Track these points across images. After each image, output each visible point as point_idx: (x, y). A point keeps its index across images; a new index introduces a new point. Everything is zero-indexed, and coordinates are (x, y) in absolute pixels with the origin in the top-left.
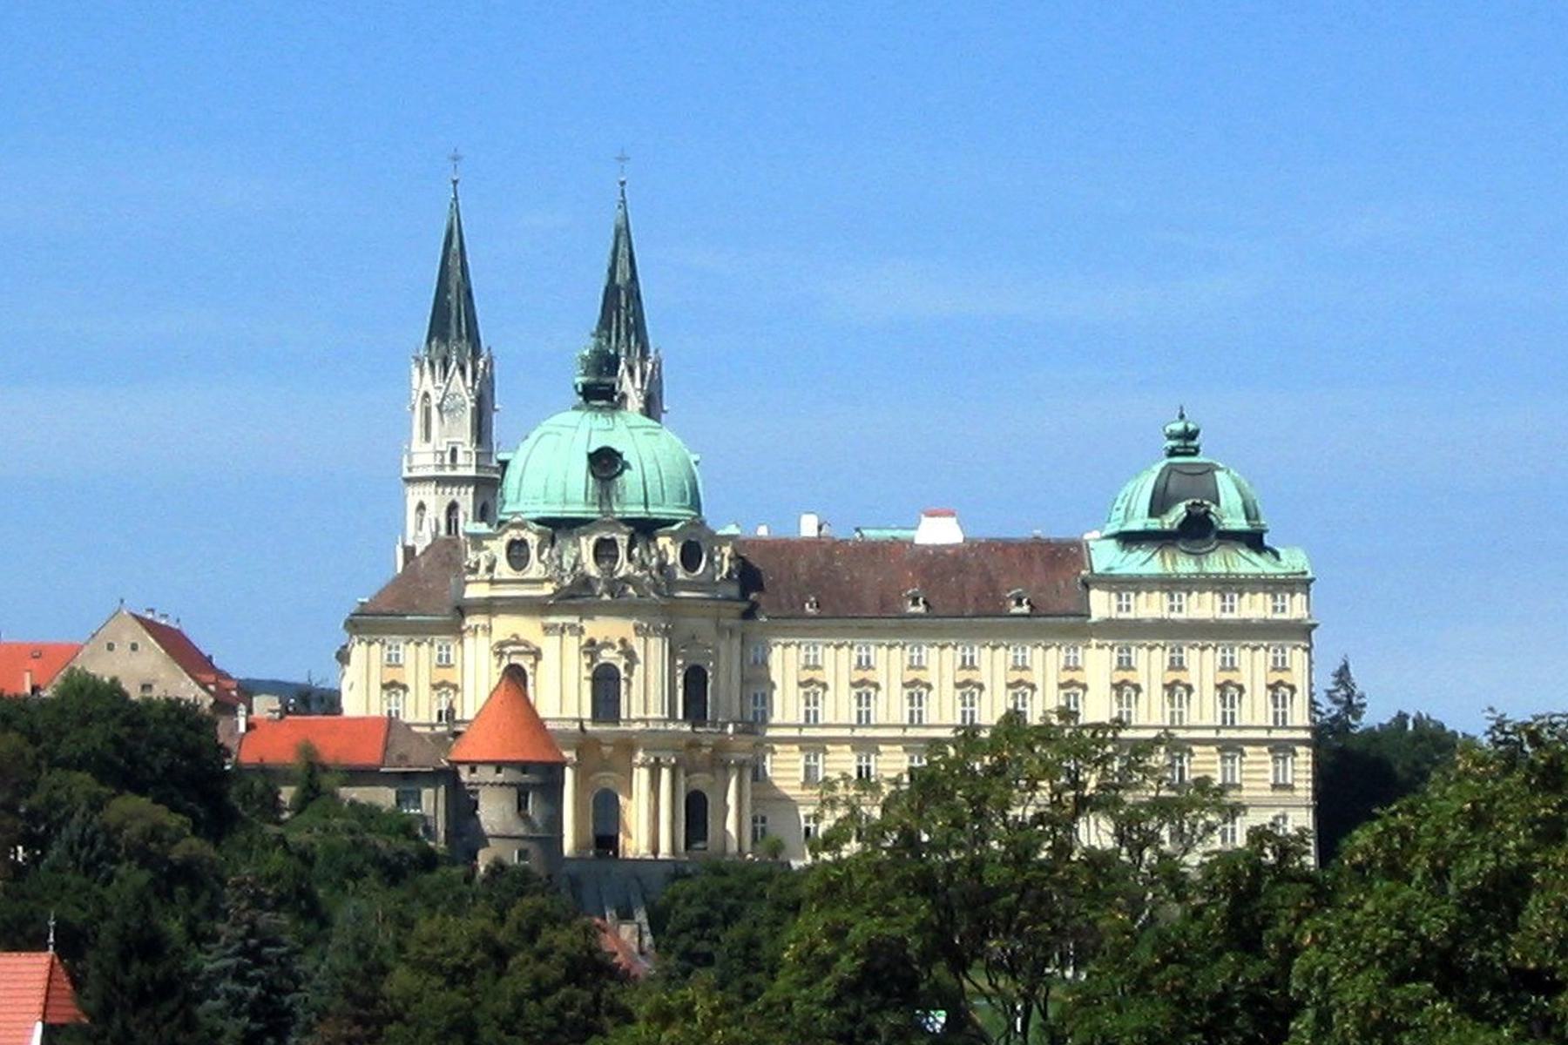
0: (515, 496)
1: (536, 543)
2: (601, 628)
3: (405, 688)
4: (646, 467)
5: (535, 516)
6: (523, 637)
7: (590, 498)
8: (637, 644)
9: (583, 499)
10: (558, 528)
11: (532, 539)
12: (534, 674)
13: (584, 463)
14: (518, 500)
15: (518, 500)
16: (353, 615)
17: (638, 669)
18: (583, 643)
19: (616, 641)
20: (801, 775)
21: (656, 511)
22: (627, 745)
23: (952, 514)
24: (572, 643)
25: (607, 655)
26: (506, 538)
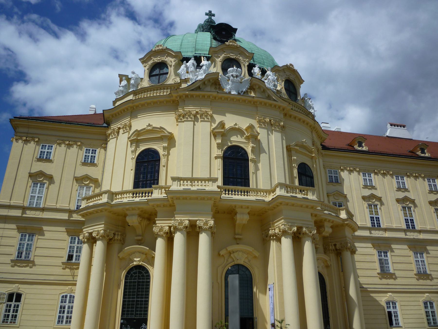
1: (173, 63)
3: (50, 178)
11: (171, 61)
17: (263, 157)
20: (377, 265)
23: (404, 126)
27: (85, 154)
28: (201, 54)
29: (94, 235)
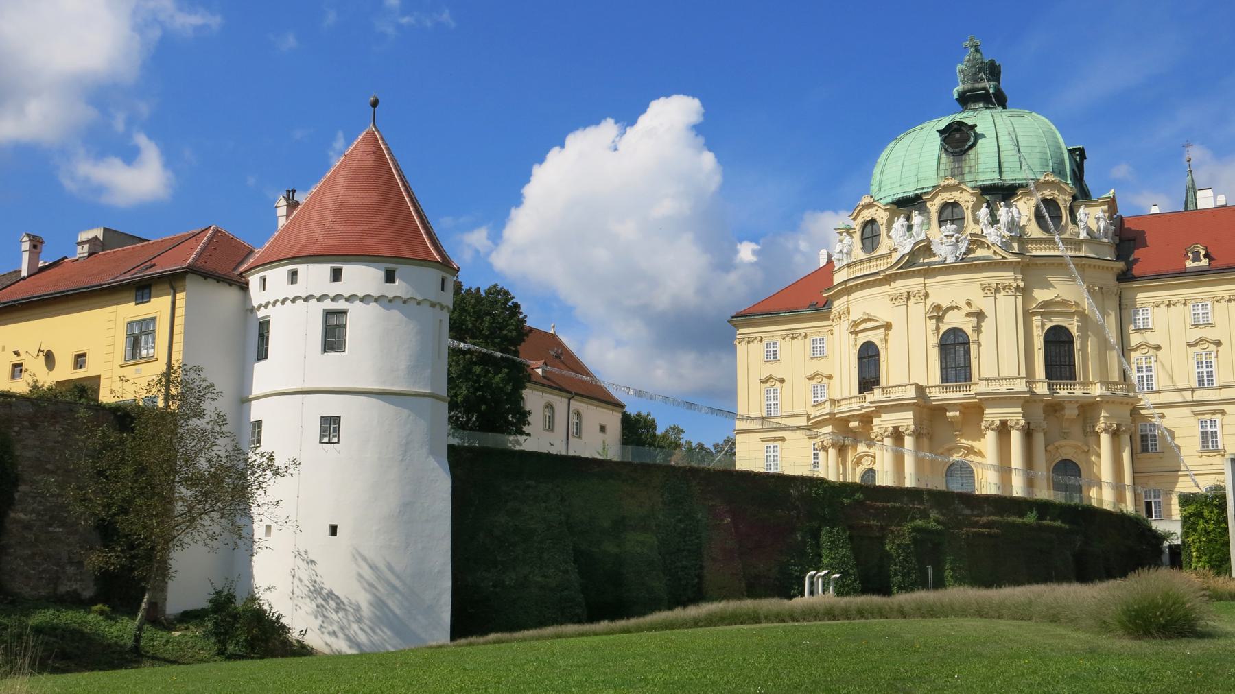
0: (877, 188)
1: (885, 220)
2: (945, 290)
4: (1006, 141)
5: (889, 200)
6: (873, 314)
7: (942, 174)
8: (983, 303)
9: (935, 172)
10: (908, 204)
11: (881, 216)
12: (886, 349)
13: (937, 139)
14: (880, 190)
15: (880, 190)
16: (733, 317)
18: (928, 307)
19: (962, 304)
21: (1009, 178)
22: (974, 412)
24: (918, 310)
25: (953, 320)
26: (860, 220)
27: (812, 346)
28: (923, 189)
29: (825, 444)
